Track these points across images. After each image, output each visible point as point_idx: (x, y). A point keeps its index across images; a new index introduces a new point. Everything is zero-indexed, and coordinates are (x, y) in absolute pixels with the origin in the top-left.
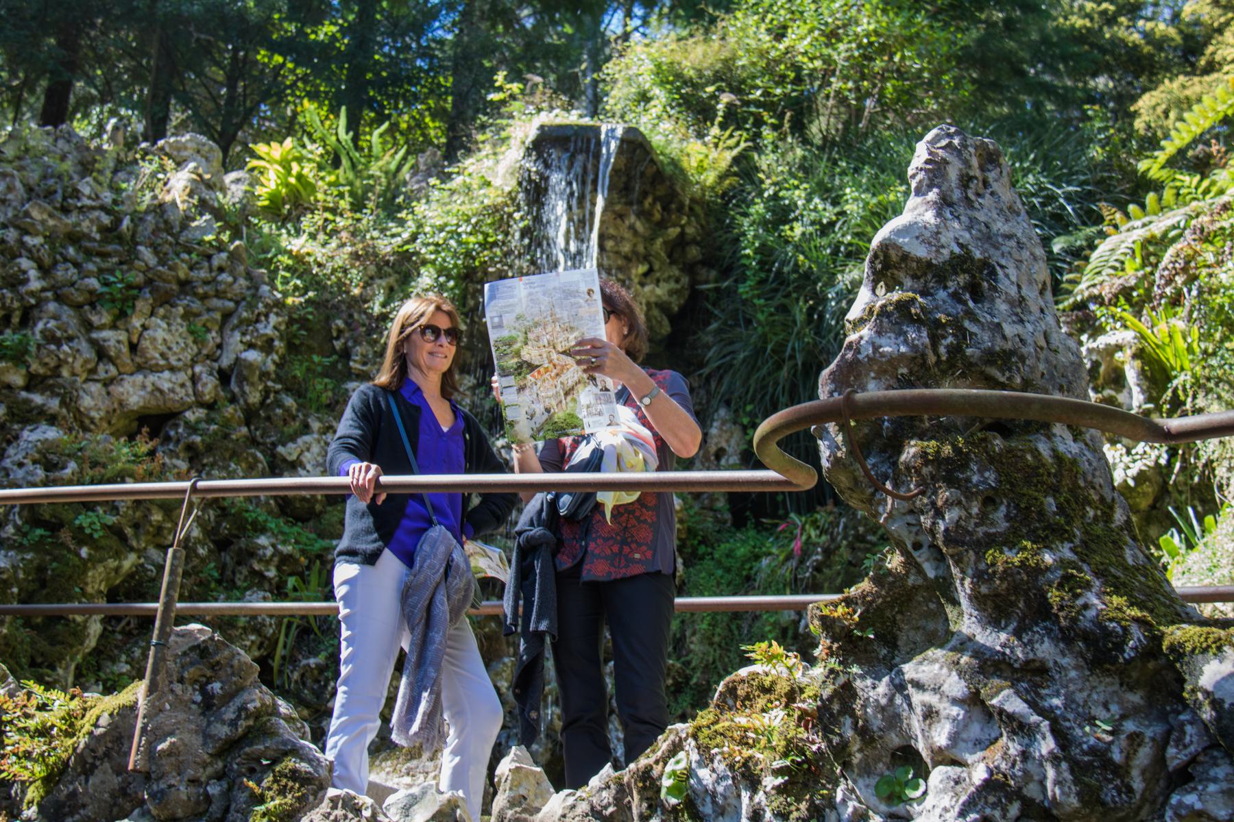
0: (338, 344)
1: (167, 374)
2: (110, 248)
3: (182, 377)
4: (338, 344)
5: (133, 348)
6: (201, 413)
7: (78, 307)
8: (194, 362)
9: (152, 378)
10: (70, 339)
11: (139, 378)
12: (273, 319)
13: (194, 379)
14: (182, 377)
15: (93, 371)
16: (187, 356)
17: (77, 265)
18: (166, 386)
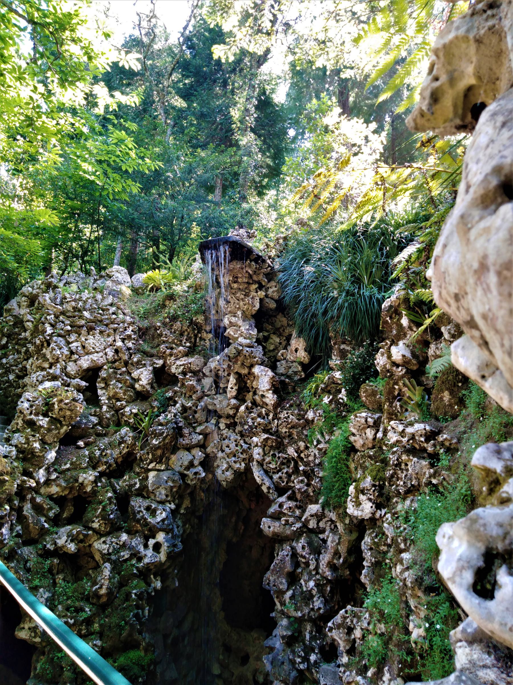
1: (96, 354)
5: (84, 347)
8: (105, 349)
9: (91, 356)
11: (86, 357)
14: (101, 354)
15: (70, 358)
17: (63, 322)
18: (95, 359)
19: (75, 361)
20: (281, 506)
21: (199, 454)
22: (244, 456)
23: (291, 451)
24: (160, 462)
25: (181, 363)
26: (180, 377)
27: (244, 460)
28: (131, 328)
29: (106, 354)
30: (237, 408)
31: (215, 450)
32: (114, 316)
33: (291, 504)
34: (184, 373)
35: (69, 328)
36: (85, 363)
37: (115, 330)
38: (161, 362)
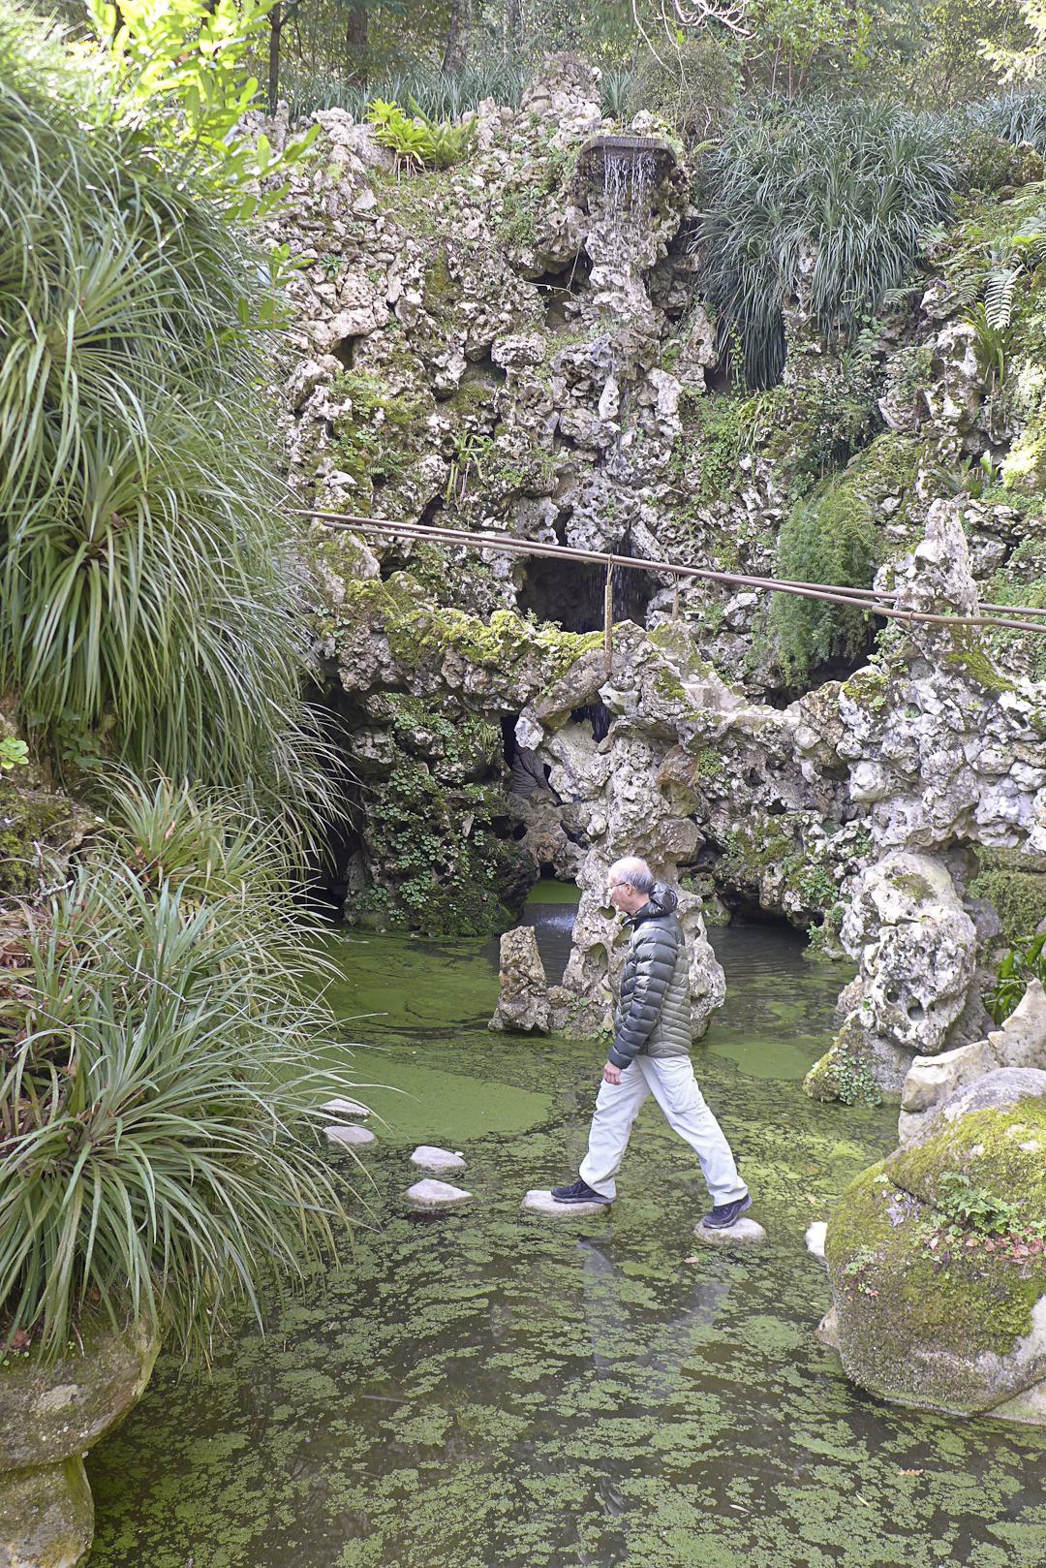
0: (453, 274)
2: (317, 224)
3: (369, 311)
4: (453, 274)
5: (338, 293)
6: (380, 333)
7: (303, 269)
9: (352, 314)
11: (343, 315)
12: (418, 265)
13: (375, 311)
14: (369, 311)
18: (359, 319)
19: (327, 321)
20: (683, 593)
21: (550, 508)
23: (705, 515)
25: (513, 345)
26: (509, 370)
28: (418, 265)
29: (375, 311)
30: (614, 438)
32: (385, 237)
33: (695, 592)
34: (513, 363)
36: (343, 326)
37: (389, 263)
38: (464, 336)
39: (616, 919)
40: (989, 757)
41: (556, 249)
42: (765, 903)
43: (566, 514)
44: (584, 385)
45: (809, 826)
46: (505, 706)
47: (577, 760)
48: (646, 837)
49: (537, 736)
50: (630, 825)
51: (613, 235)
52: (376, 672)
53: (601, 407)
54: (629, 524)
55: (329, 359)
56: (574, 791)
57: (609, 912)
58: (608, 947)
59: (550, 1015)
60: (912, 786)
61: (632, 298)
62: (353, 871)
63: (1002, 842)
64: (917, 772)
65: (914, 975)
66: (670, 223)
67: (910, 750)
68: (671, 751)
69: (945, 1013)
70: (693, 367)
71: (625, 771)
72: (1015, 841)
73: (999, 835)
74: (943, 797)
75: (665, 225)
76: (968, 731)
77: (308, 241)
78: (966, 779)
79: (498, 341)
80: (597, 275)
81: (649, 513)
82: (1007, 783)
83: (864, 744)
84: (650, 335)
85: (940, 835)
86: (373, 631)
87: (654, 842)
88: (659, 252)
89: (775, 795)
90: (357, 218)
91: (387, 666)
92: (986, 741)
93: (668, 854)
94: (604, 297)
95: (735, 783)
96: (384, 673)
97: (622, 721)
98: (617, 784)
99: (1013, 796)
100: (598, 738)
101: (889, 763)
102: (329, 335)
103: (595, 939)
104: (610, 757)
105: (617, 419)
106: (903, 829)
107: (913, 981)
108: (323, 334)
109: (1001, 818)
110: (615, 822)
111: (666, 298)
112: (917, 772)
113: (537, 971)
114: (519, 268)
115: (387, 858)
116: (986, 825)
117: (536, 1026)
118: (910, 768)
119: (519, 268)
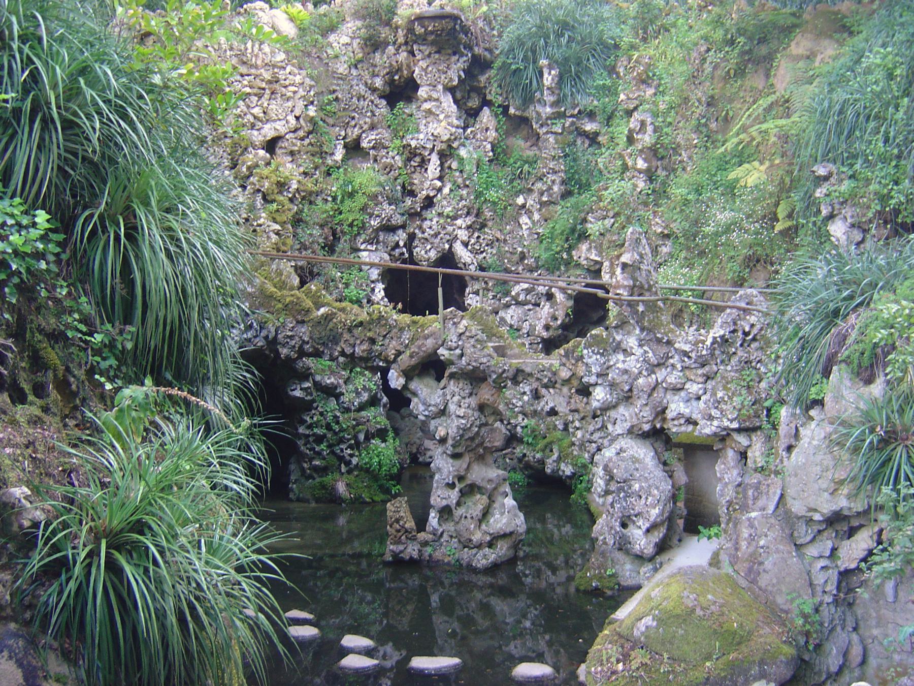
1: (278, 122)
5: (264, 113)
6: (291, 135)
10: (245, 115)
16: (284, 114)
22: (448, 237)
24: (372, 244)
25: (373, 137)
27: (448, 241)
29: (287, 122)
30: (440, 190)
31: (417, 231)
34: (373, 148)
35: (248, 90)
36: (269, 131)
37: (295, 92)
39: (457, 489)
40: (672, 379)
41: (396, 77)
42: (548, 471)
43: (412, 237)
44: (418, 159)
45: (573, 422)
46: (381, 364)
47: (427, 395)
48: (472, 439)
49: (402, 381)
50: (461, 432)
51: (430, 69)
52: (301, 347)
53: (429, 171)
54: (451, 242)
55: (262, 153)
56: (426, 413)
57: (452, 486)
58: (453, 507)
59: (420, 551)
60: (628, 398)
61: (444, 105)
62: (292, 467)
63: (683, 429)
64: (630, 390)
65: (636, 512)
66: (465, 58)
67: (626, 377)
68: (483, 385)
69: (656, 533)
70: (485, 143)
71: (456, 399)
72: (690, 428)
73: (681, 425)
74: (646, 404)
75: (462, 60)
76: (658, 365)
77: (245, 83)
78: (658, 395)
79: (364, 135)
80: (422, 92)
81: (463, 235)
82: (683, 394)
83: (599, 375)
84: (457, 127)
85: (646, 427)
86: (298, 322)
87: (477, 441)
88: (459, 77)
89: (551, 405)
90: (274, 66)
91: (308, 343)
92: (668, 369)
93: (485, 448)
94: (426, 106)
95: (526, 398)
96: (306, 347)
97: (453, 369)
98: (452, 407)
99: (688, 401)
100: (439, 379)
101: (613, 385)
102: (261, 138)
103: (444, 503)
104: (447, 391)
105: (440, 178)
106: (625, 425)
107: (636, 516)
108: (257, 137)
109: (680, 416)
110: (453, 431)
111: (465, 103)
112: (630, 390)
113: (410, 524)
114: (374, 90)
115: (314, 458)
116: (673, 420)
117: (411, 558)
118: (627, 388)
119: (374, 90)
